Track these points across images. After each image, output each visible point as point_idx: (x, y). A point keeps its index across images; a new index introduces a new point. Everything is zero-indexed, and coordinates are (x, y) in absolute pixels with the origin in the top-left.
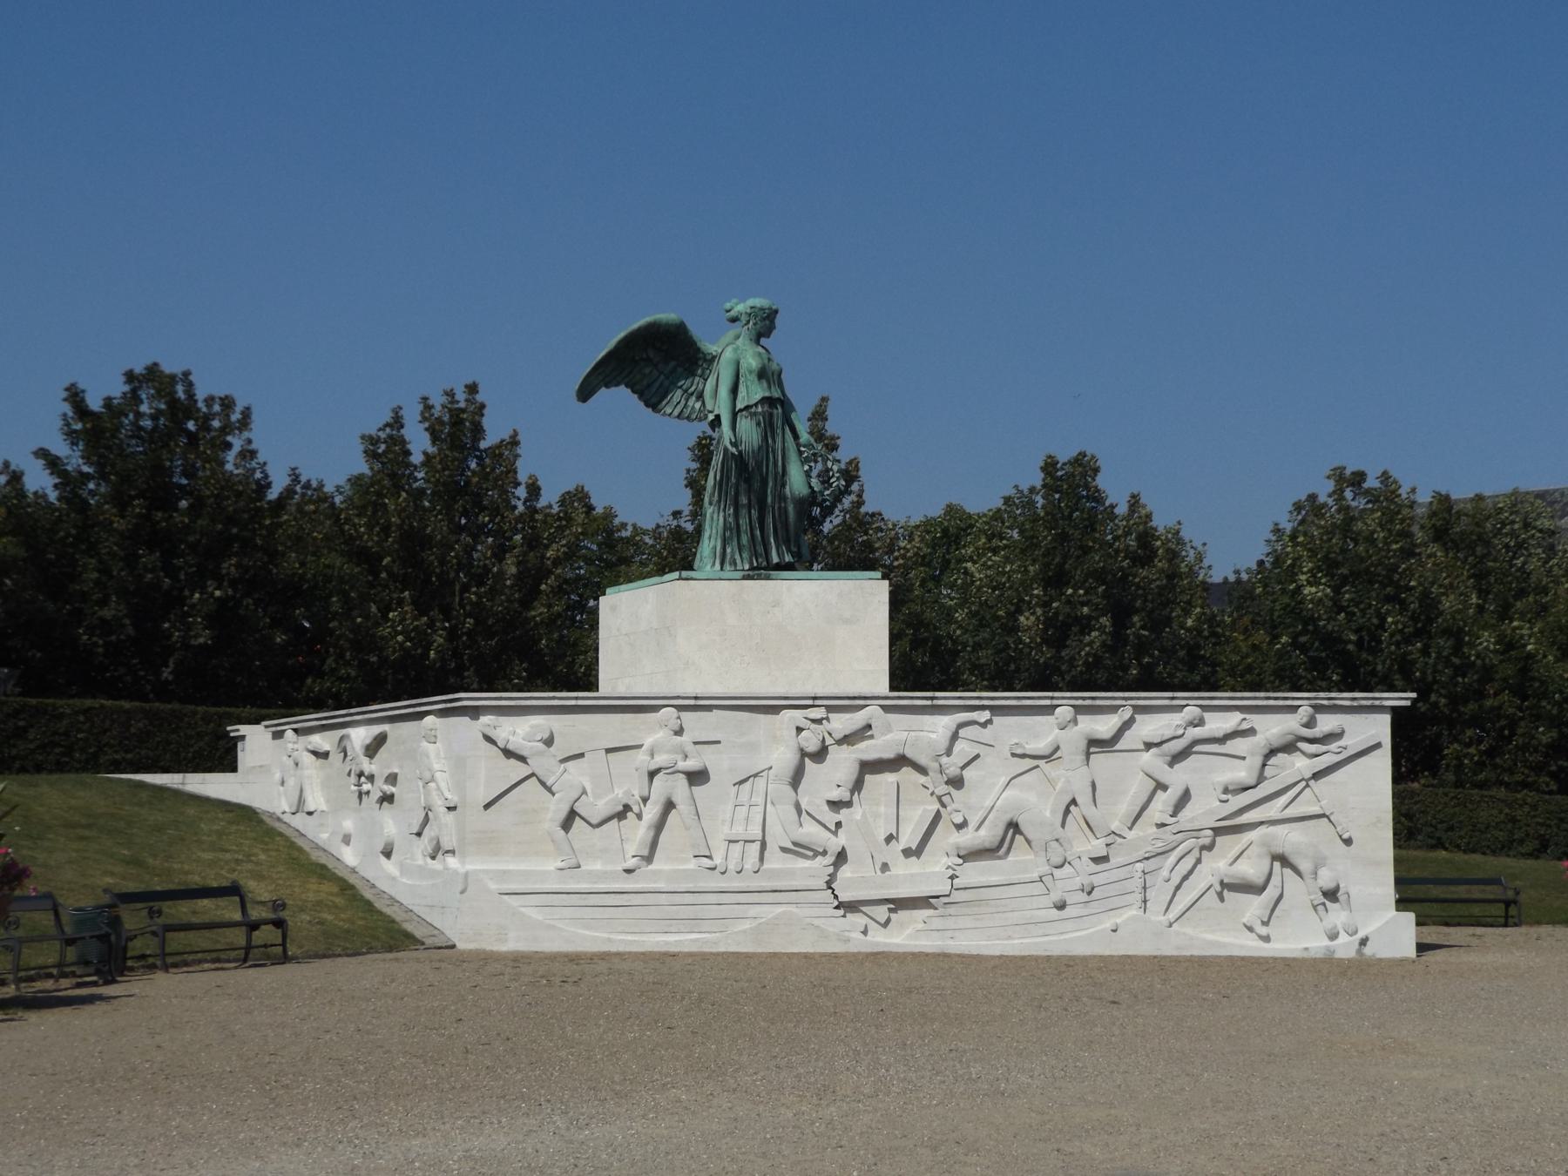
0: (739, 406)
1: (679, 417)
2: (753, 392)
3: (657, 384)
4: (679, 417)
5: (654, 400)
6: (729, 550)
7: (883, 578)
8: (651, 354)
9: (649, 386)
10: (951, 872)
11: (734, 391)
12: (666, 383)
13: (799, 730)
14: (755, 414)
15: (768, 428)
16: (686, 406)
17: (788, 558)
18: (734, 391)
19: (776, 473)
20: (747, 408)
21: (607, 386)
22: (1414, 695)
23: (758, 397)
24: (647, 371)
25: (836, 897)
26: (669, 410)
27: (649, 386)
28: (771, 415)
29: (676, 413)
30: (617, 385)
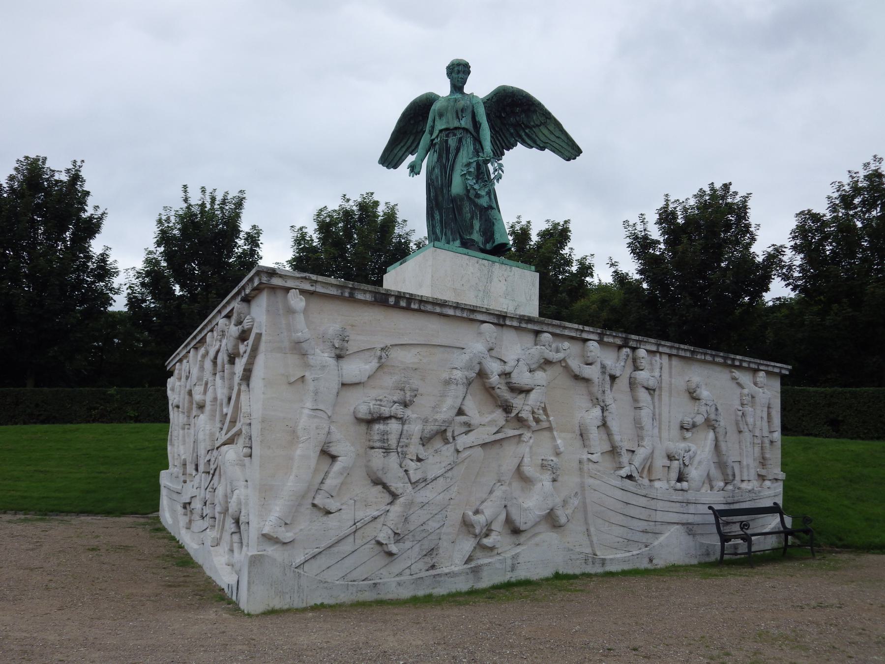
28: (447, 141)
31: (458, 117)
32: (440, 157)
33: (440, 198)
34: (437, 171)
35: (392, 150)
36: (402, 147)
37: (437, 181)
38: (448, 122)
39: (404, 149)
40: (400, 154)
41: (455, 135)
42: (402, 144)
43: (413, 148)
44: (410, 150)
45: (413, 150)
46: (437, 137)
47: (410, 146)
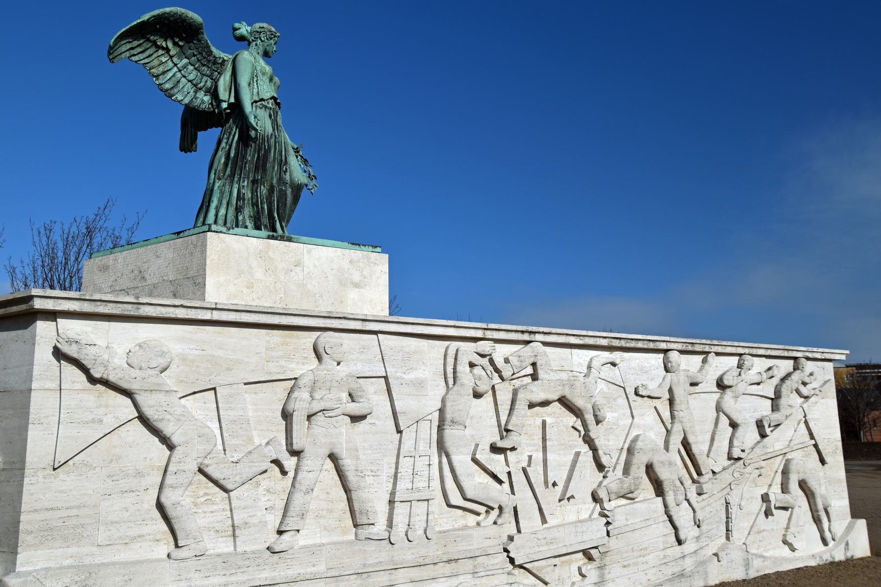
3: (170, 74)
6: (240, 218)
7: (383, 252)
8: (170, 45)
9: (164, 73)
10: (604, 520)
12: (179, 75)
13: (472, 365)
14: (266, 107)
16: (195, 98)
19: (281, 160)
22: (848, 352)
24: (164, 59)
25: (512, 561)
27: (164, 73)
32: (274, 130)
34: (273, 141)
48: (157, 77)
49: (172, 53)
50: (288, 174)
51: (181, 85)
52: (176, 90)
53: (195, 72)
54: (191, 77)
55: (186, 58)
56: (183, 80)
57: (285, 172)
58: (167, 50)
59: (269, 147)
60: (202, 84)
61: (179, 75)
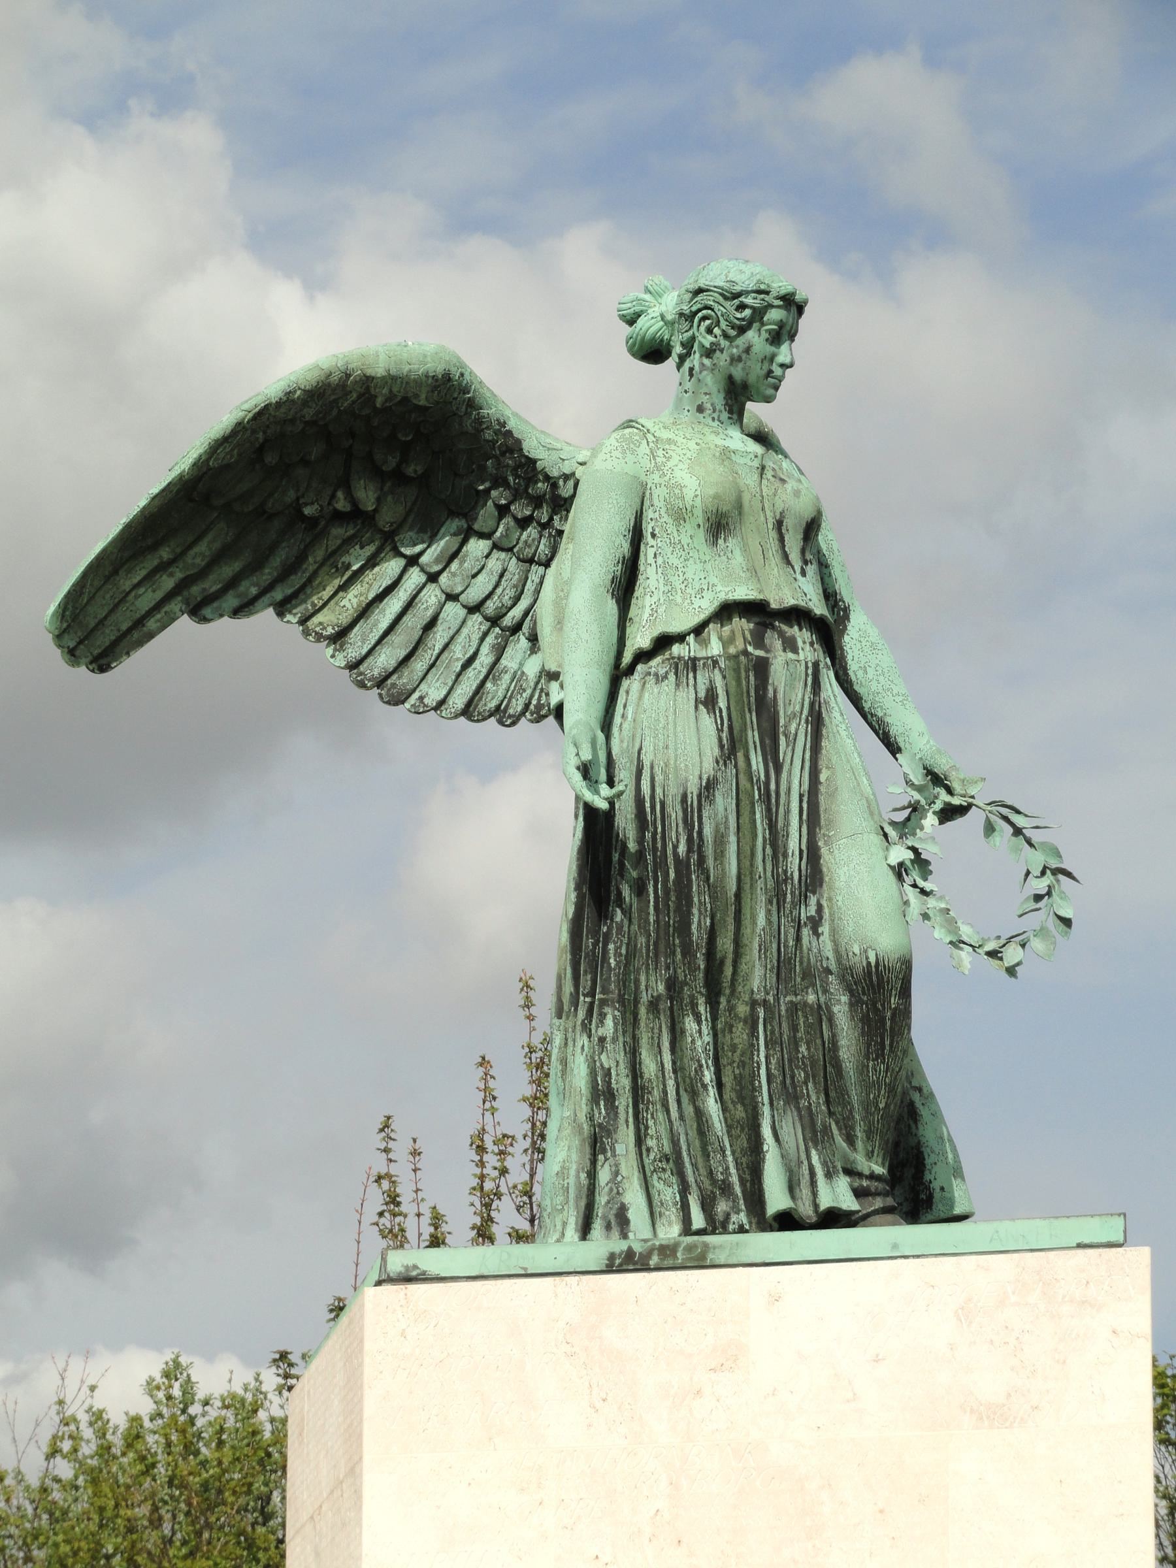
0: (640, 639)
1: (468, 711)
2: (685, 587)
3: (394, 605)
4: (468, 711)
5: (385, 659)
6: (604, 1175)
8: (367, 496)
9: (364, 612)
11: (625, 585)
12: (431, 596)
15: (751, 717)
17: (837, 1194)
18: (625, 585)
19: (781, 881)
20: (663, 642)
21: (197, 611)
23: (707, 605)
26: (433, 691)
27: (364, 612)
28: (762, 668)
29: (458, 700)
30: (242, 609)
31: (786, 557)
32: (731, 748)
33: (725, 944)
35: (115, 572)
36: (163, 567)
37: (720, 855)
38: (754, 572)
39: (168, 583)
40: (146, 599)
41: (790, 645)
42: (165, 554)
43: (211, 585)
44: (195, 590)
45: (209, 599)
46: (699, 630)
47: (203, 573)
48: (340, 637)
49: (386, 519)
50: (825, 929)
51: (439, 637)
52: (419, 665)
53: (495, 563)
54: (474, 594)
55: (453, 514)
56: (454, 612)
57: (815, 923)
58: (357, 515)
59: (696, 844)
60: (517, 612)
61: (431, 596)
